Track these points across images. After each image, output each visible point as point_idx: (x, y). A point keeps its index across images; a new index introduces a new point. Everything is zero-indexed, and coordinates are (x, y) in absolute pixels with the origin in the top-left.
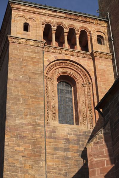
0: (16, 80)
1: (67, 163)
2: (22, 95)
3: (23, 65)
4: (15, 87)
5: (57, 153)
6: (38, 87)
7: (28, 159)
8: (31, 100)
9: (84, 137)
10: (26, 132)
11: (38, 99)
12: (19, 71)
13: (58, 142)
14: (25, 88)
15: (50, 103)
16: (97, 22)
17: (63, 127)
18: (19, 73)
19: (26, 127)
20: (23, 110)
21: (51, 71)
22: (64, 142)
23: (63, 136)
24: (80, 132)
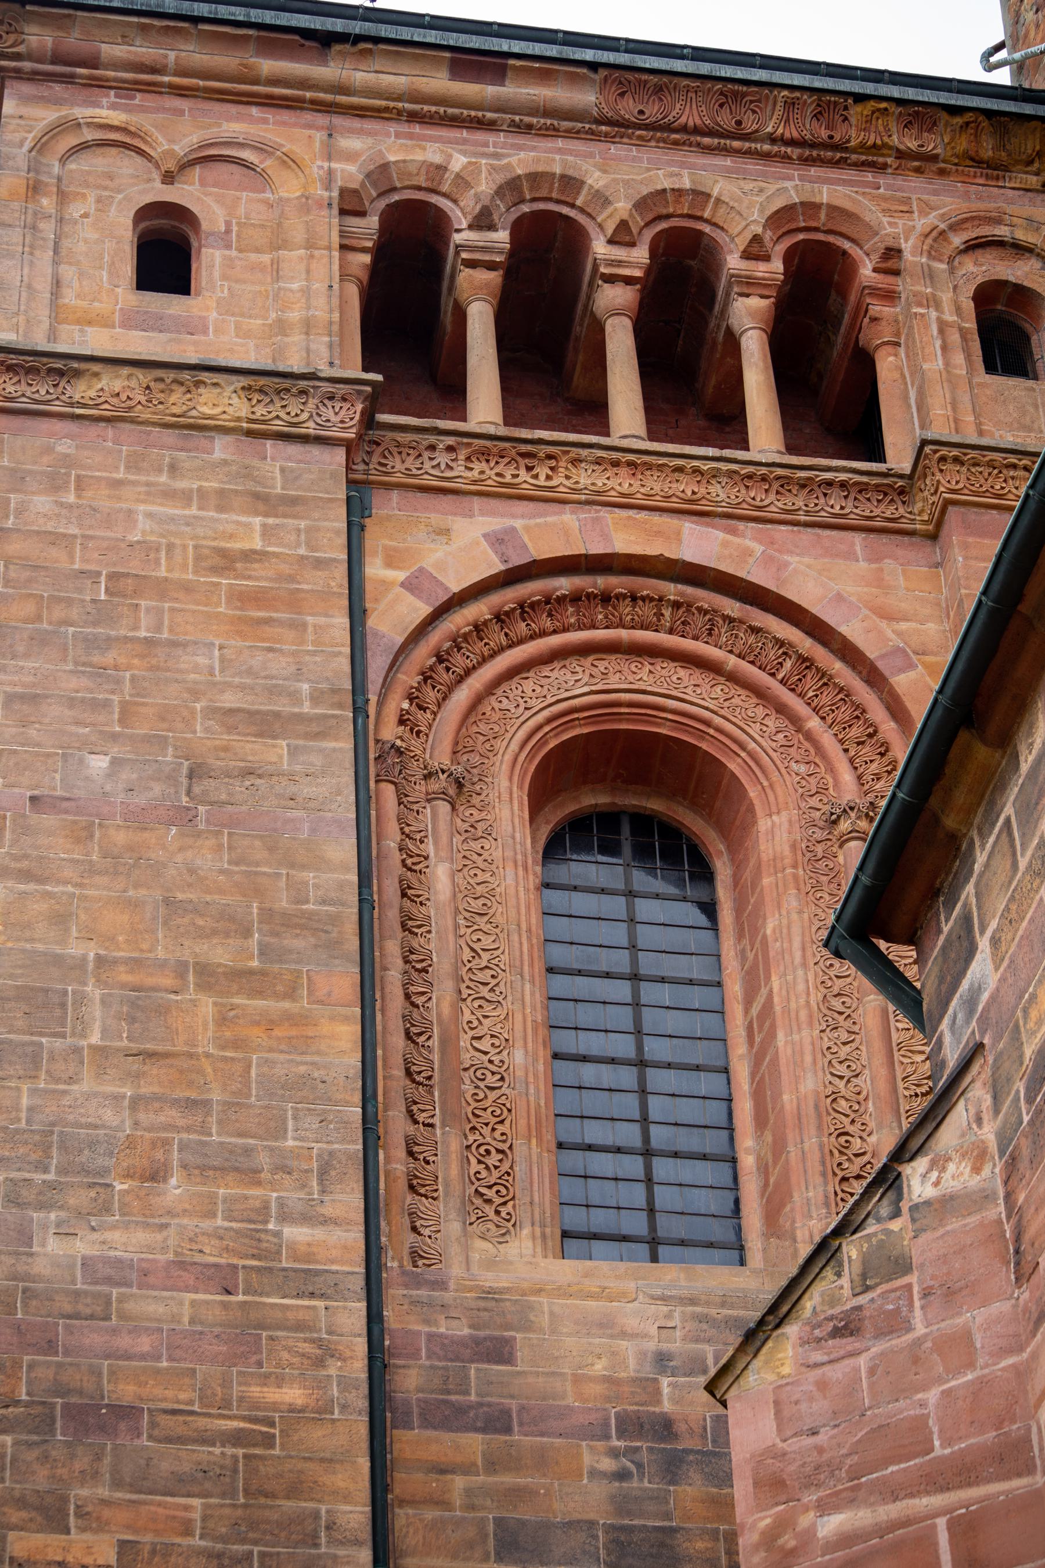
0: (33, 799)
2: (100, 960)
3: (127, 639)
4: (27, 876)
6: (292, 865)
8: (207, 1006)
11: (291, 994)
12: (71, 702)
13: (542, 1461)
14: (136, 886)
15: (448, 1043)
16: (963, 144)
17: (590, 1296)
21: (462, 696)
22: (607, 1464)
23: (598, 1389)
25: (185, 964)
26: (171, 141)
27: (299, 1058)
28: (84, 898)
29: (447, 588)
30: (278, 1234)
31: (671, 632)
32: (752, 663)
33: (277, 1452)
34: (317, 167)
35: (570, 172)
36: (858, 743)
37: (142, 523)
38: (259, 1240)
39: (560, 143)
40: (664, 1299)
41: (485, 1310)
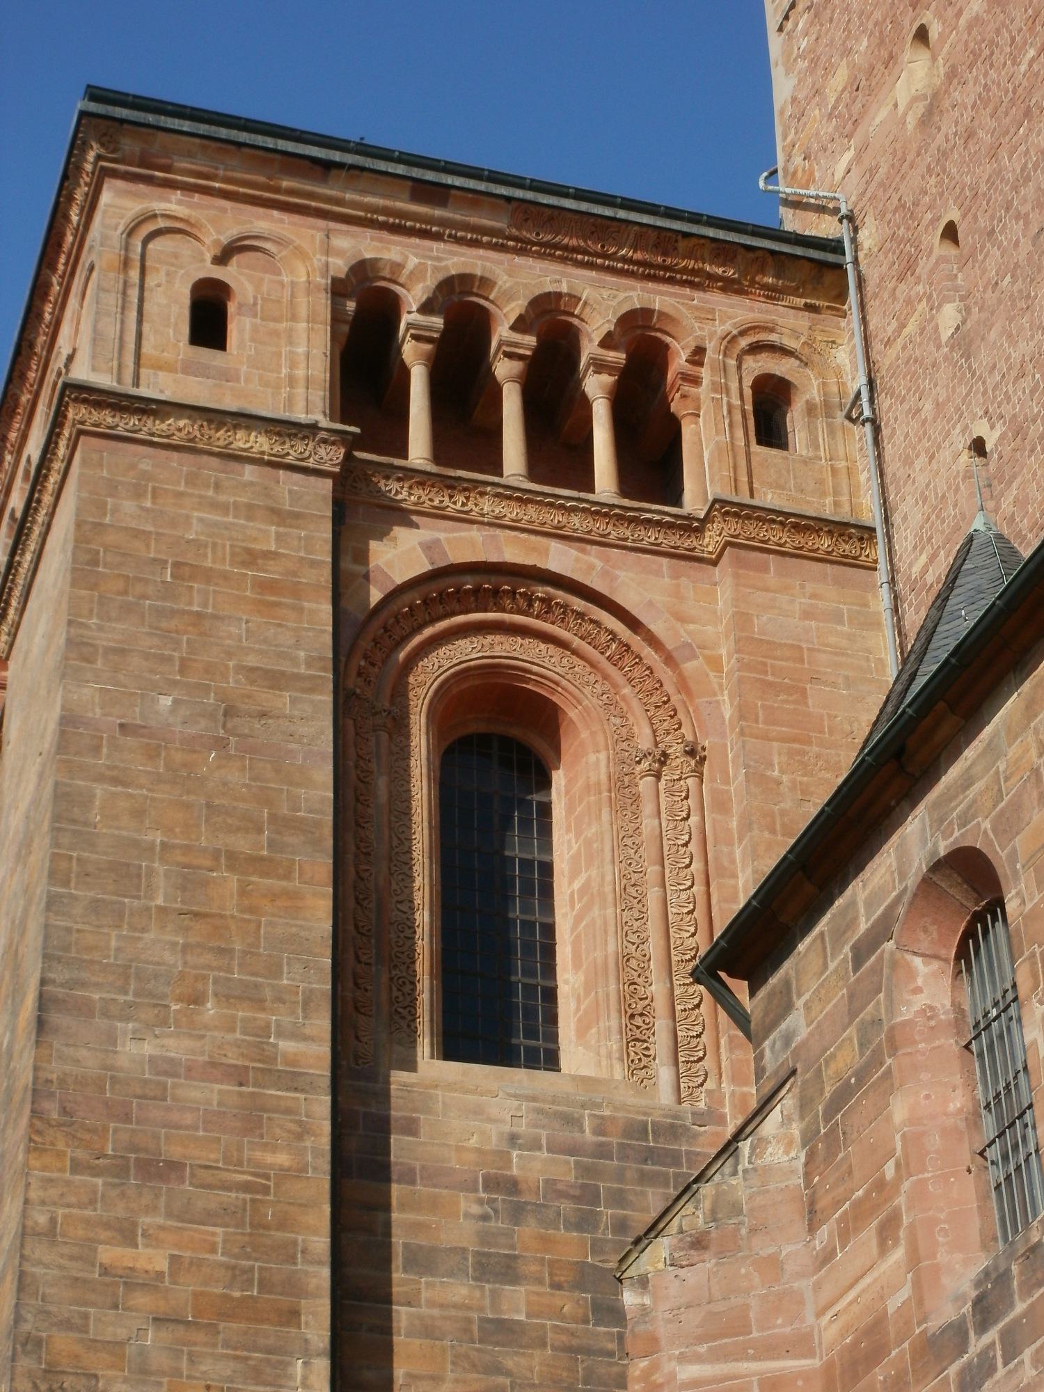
0: (122, 726)
1: (498, 1369)
2: (163, 844)
3: (184, 612)
4: (116, 781)
5: (425, 1295)
7: (200, 1337)
8: (233, 881)
9: (632, 1168)
10: (187, 1128)
11: (287, 876)
12: (147, 656)
13: (434, 1205)
14: (189, 792)
18: (152, 671)
19: (195, 1094)
20: (168, 957)
22: (476, 1209)
24: (599, 1130)
25: (219, 851)
26: (219, 233)
27: (292, 922)
28: (153, 799)
29: (393, 581)
30: (275, 1046)
31: (537, 617)
32: (589, 643)
33: (271, 1198)
34: (318, 259)
35: (487, 275)
36: (656, 707)
37: (195, 526)
38: (263, 1050)
39: (481, 252)
40: (516, 1096)
41: (402, 1098)
